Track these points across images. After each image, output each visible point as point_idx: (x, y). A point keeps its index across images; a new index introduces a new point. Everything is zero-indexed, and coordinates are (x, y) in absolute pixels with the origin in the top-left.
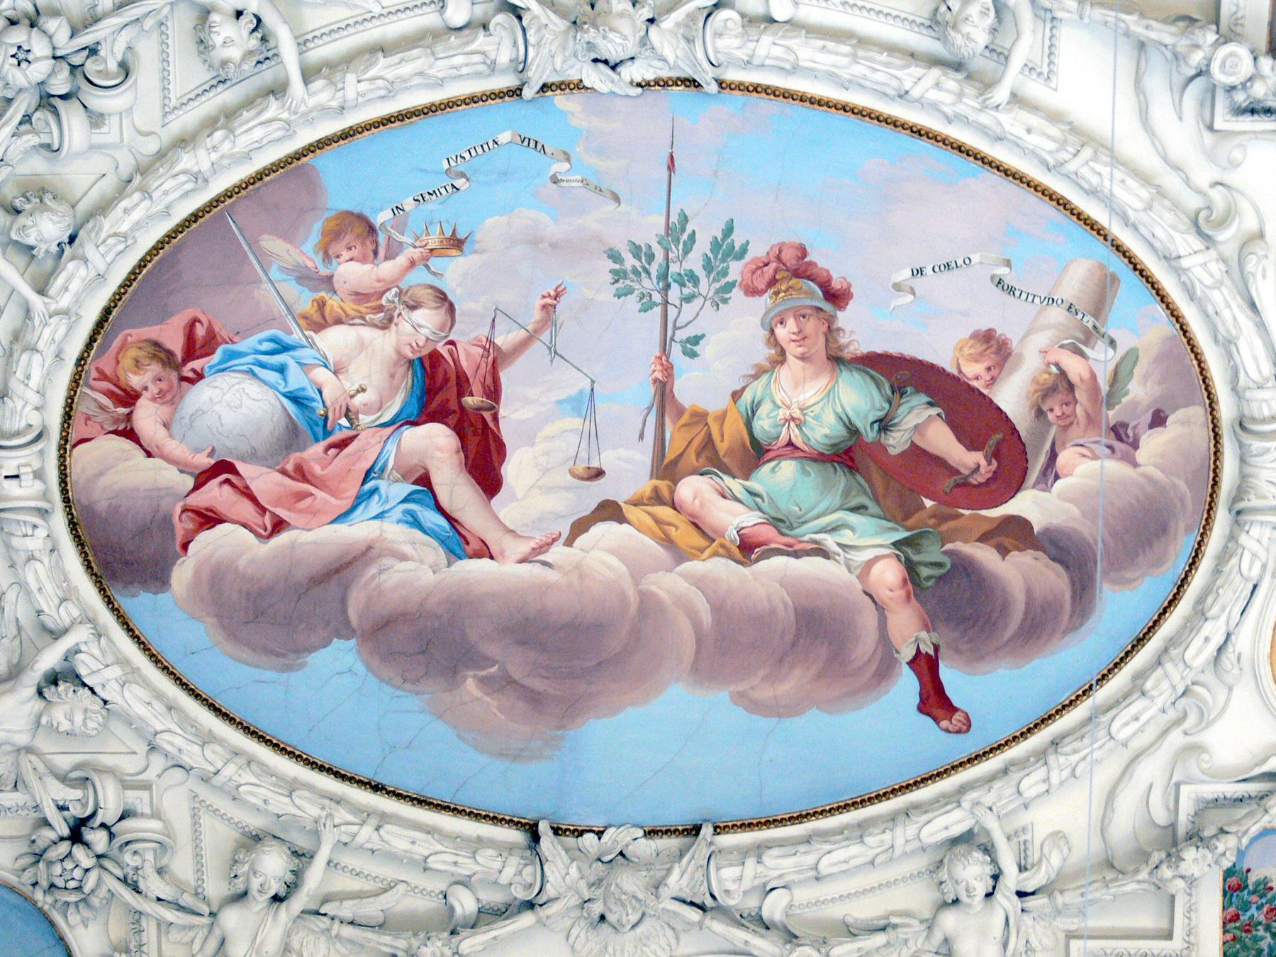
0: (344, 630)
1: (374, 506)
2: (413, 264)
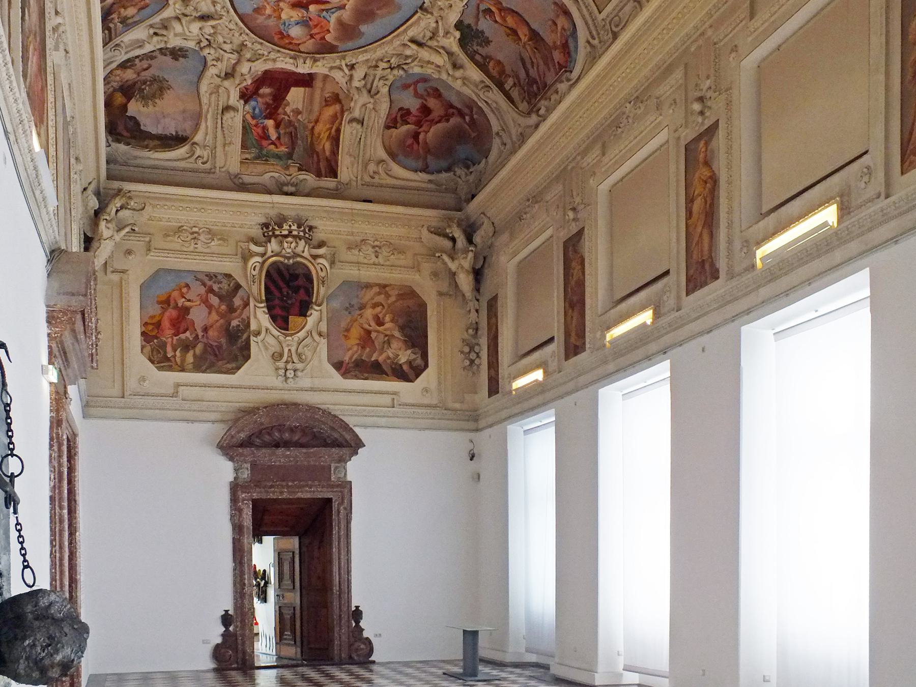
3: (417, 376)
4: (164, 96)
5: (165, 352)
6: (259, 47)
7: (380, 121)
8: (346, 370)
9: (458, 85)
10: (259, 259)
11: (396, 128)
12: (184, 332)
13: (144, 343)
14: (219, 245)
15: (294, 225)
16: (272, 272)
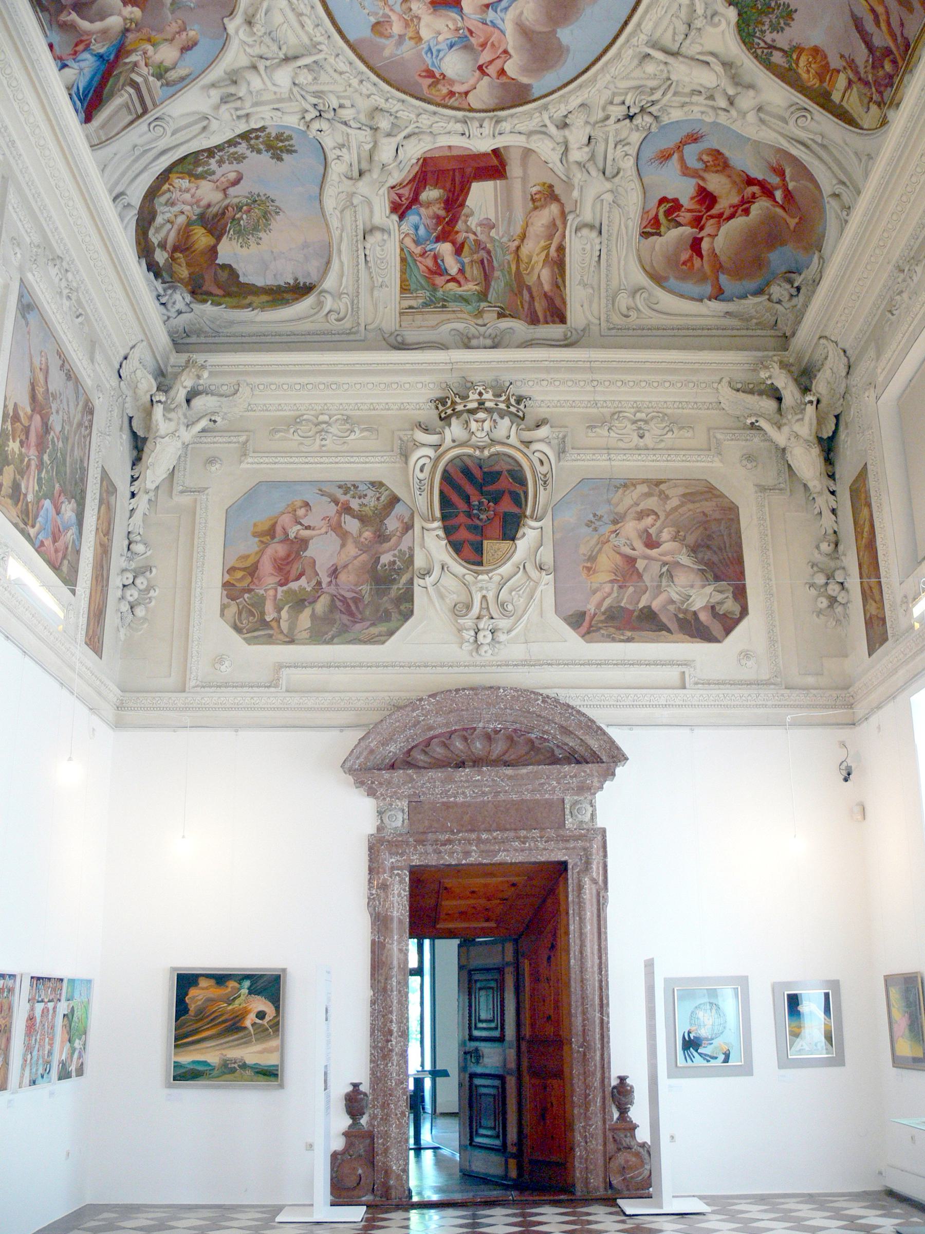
0: (554, 32)
1: (499, 22)
2: (392, 10)
3: (728, 631)
4: (271, 227)
5: (263, 613)
6: (399, 106)
7: (630, 224)
8: (591, 626)
9: (750, 128)
10: (430, 452)
11: (659, 235)
12: (298, 578)
13: (226, 601)
14: (363, 438)
15: (487, 392)
16: (451, 470)
